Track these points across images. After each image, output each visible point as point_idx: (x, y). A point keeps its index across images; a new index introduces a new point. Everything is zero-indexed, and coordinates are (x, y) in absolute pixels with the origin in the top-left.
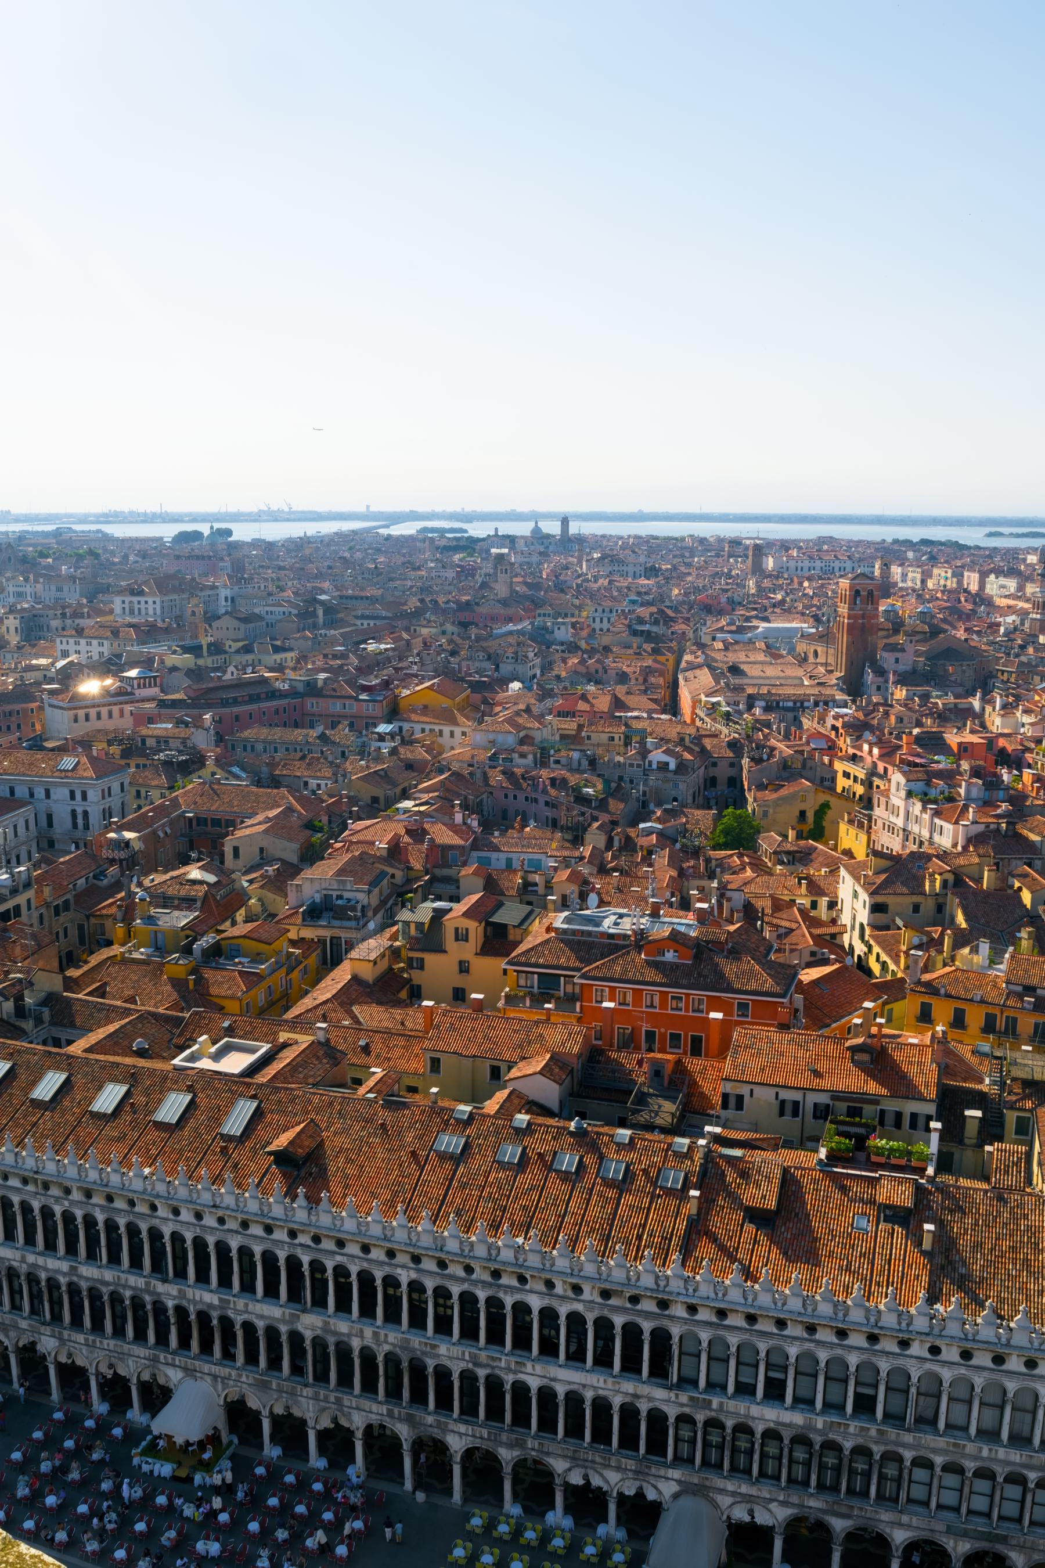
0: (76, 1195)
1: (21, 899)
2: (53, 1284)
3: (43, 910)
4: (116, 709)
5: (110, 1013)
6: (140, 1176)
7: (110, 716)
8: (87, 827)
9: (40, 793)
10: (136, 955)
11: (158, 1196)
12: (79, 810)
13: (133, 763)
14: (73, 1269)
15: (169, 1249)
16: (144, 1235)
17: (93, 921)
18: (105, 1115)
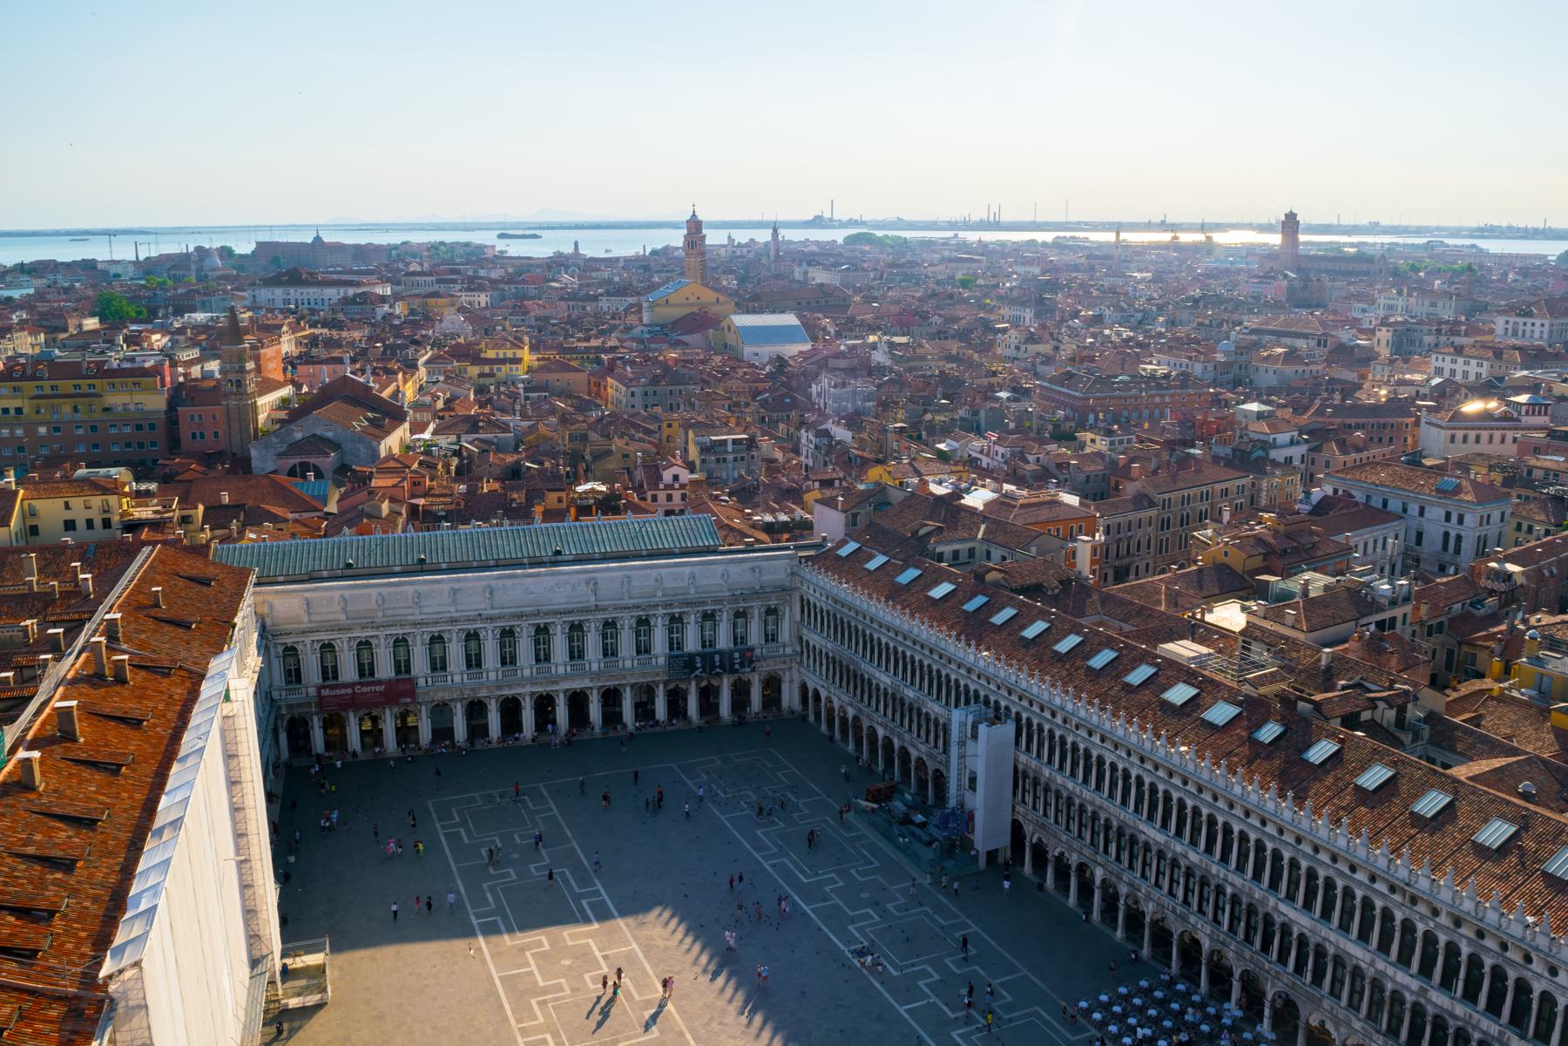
0: (1444, 919)
1: (1398, 612)
2: (1397, 997)
3: (1416, 627)
4: (1497, 434)
5: (1494, 748)
6: (1520, 922)
7: (1503, 441)
8: (1458, 551)
9: (1414, 509)
10: (1515, 694)
11: (1537, 949)
12: (1453, 534)
13: (1514, 493)
14: (1423, 991)
15: (1535, 1006)
16: (1510, 983)
17: (1465, 648)
18: (1488, 848)
